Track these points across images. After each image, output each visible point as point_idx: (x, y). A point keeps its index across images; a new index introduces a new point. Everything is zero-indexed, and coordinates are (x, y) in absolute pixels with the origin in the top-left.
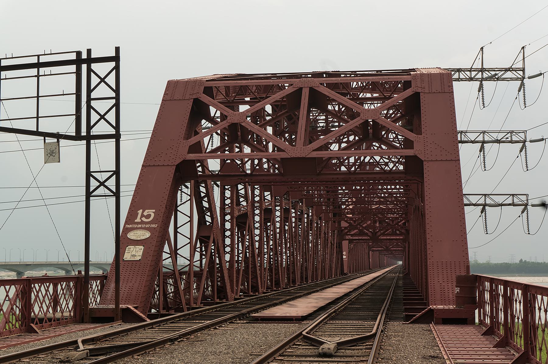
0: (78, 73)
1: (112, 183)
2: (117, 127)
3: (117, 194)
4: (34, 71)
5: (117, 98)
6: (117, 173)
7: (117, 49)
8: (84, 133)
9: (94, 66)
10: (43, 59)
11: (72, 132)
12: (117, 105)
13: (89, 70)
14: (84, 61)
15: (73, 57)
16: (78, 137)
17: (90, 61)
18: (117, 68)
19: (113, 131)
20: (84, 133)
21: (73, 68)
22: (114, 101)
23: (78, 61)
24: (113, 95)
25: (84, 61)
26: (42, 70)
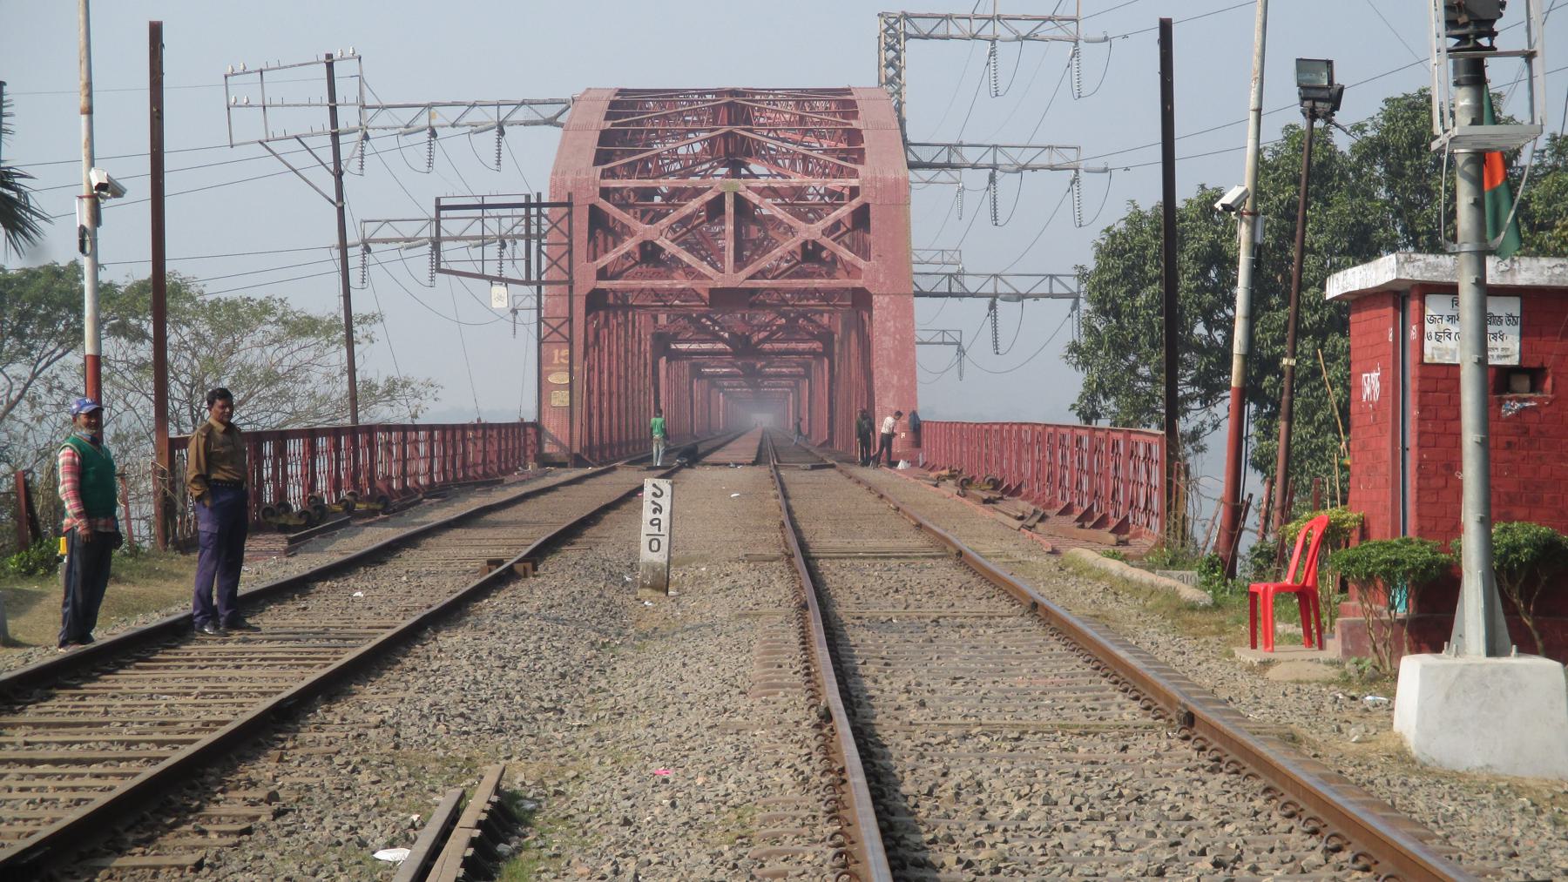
0: (528, 217)
1: (565, 330)
2: (570, 273)
3: (570, 342)
4: (478, 212)
5: (570, 244)
6: (571, 321)
7: (570, 195)
8: (534, 277)
10: (488, 201)
11: (522, 277)
12: (570, 252)
14: (534, 205)
15: (522, 200)
16: (527, 282)
17: (539, 205)
18: (570, 214)
19: (566, 277)
20: (534, 277)
21: (522, 211)
23: (527, 205)
24: (566, 240)
25: (534, 205)
26: (487, 212)
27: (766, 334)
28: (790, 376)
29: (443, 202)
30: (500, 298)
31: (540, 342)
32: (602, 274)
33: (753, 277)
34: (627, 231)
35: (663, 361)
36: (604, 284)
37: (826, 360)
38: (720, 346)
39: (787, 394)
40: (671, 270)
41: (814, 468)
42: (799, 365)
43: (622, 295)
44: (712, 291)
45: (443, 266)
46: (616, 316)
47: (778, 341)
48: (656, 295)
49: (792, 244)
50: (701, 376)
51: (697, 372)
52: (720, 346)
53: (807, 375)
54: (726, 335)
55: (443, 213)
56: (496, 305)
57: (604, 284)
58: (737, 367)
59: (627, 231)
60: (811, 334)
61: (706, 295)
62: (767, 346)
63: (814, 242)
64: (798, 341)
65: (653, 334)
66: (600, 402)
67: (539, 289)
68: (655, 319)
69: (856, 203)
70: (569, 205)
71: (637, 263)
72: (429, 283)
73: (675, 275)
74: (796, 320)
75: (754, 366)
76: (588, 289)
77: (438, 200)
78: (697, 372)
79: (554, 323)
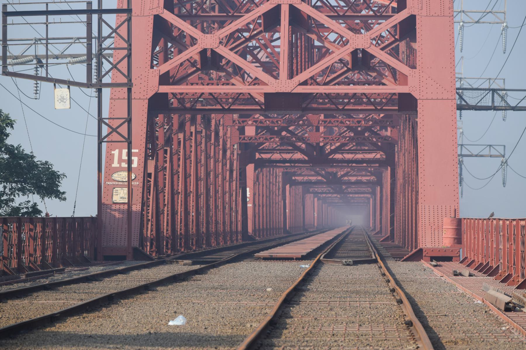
0: (89, 25)
2: (129, 76)
5: (129, 49)
6: (129, 121)
8: (94, 81)
9: (105, 16)
10: (51, 8)
11: (84, 80)
12: (129, 56)
13: (100, 20)
14: (95, 12)
15: (84, 7)
16: (89, 85)
17: (101, 11)
18: (129, 20)
19: (125, 81)
20: (94, 81)
21: (84, 17)
22: (125, 52)
23: (89, 12)
24: (125, 45)
25: (95, 12)
26: (51, 18)
27: (338, 144)
28: (368, 183)
29: (10, 9)
30: (62, 100)
31: (100, 141)
32: (165, 79)
33: (305, 83)
34: (194, 41)
35: (250, 168)
36: (164, 89)
37: (389, 168)
38: (298, 156)
39: (368, 199)
40: (229, 76)
41: (356, 263)
42: (372, 174)
43: (181, 98)
44: (267, 95)
45: (10, 69)
46: (193, 121)
47: (350, 151)
48: (216, 99)
49: (344, 53)
50: (294, 183)
51: (288, 179)
52: (298, 156)
53: (380, 182)
54: (304, 146)
55: (10, 19)
56: (59, 106)
57: (164, 89)
58: (322, 176)
59: (194, 41)
60: (375, 144)
61: (262, 100)
62: (338, 156)
63: (364, 51)
64: (364, 151)
65: (240, 144)
66: (259, 209)
67: (100, 91)
68: (242, 131)
69: (403, 15)
70: (129, 11)
71: (198, 70)
72: (34, 96)
73: (233, 81)
74: (363, 132)
75: (336, 174)
76: (151, 94)
77: (5, 6)
78: (288, 179)
79: (115, 124)
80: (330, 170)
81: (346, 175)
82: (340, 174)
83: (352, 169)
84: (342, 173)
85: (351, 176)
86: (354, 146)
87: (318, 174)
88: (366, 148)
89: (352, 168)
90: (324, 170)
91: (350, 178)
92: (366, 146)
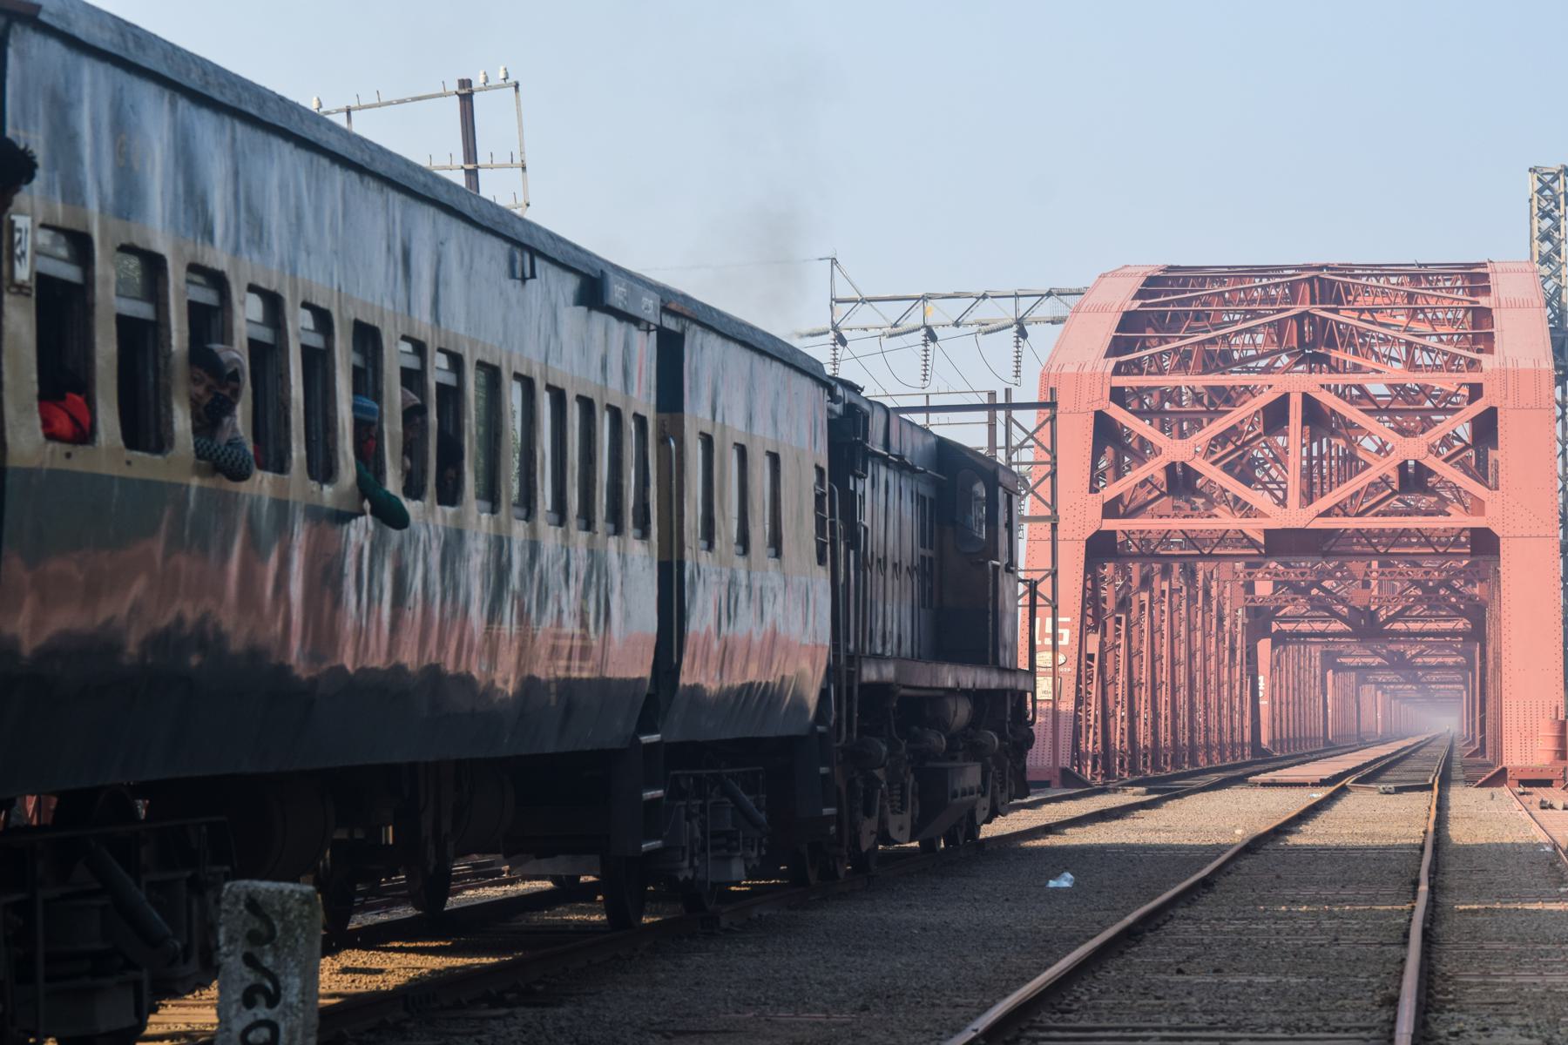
75: (1403, 654)
80: (1393, 647)
81: (1420, 654)
82: (1409, 654)
83: (1428, 647)
84: (1414, 652)
85: (1427, 655)
86: (1425, 610)
87: (1376, 654)
88: (1444, 613)
89: (1430, 645)
90: (1385, 648)
91: (1426, 660)
92: (1444, 610)
